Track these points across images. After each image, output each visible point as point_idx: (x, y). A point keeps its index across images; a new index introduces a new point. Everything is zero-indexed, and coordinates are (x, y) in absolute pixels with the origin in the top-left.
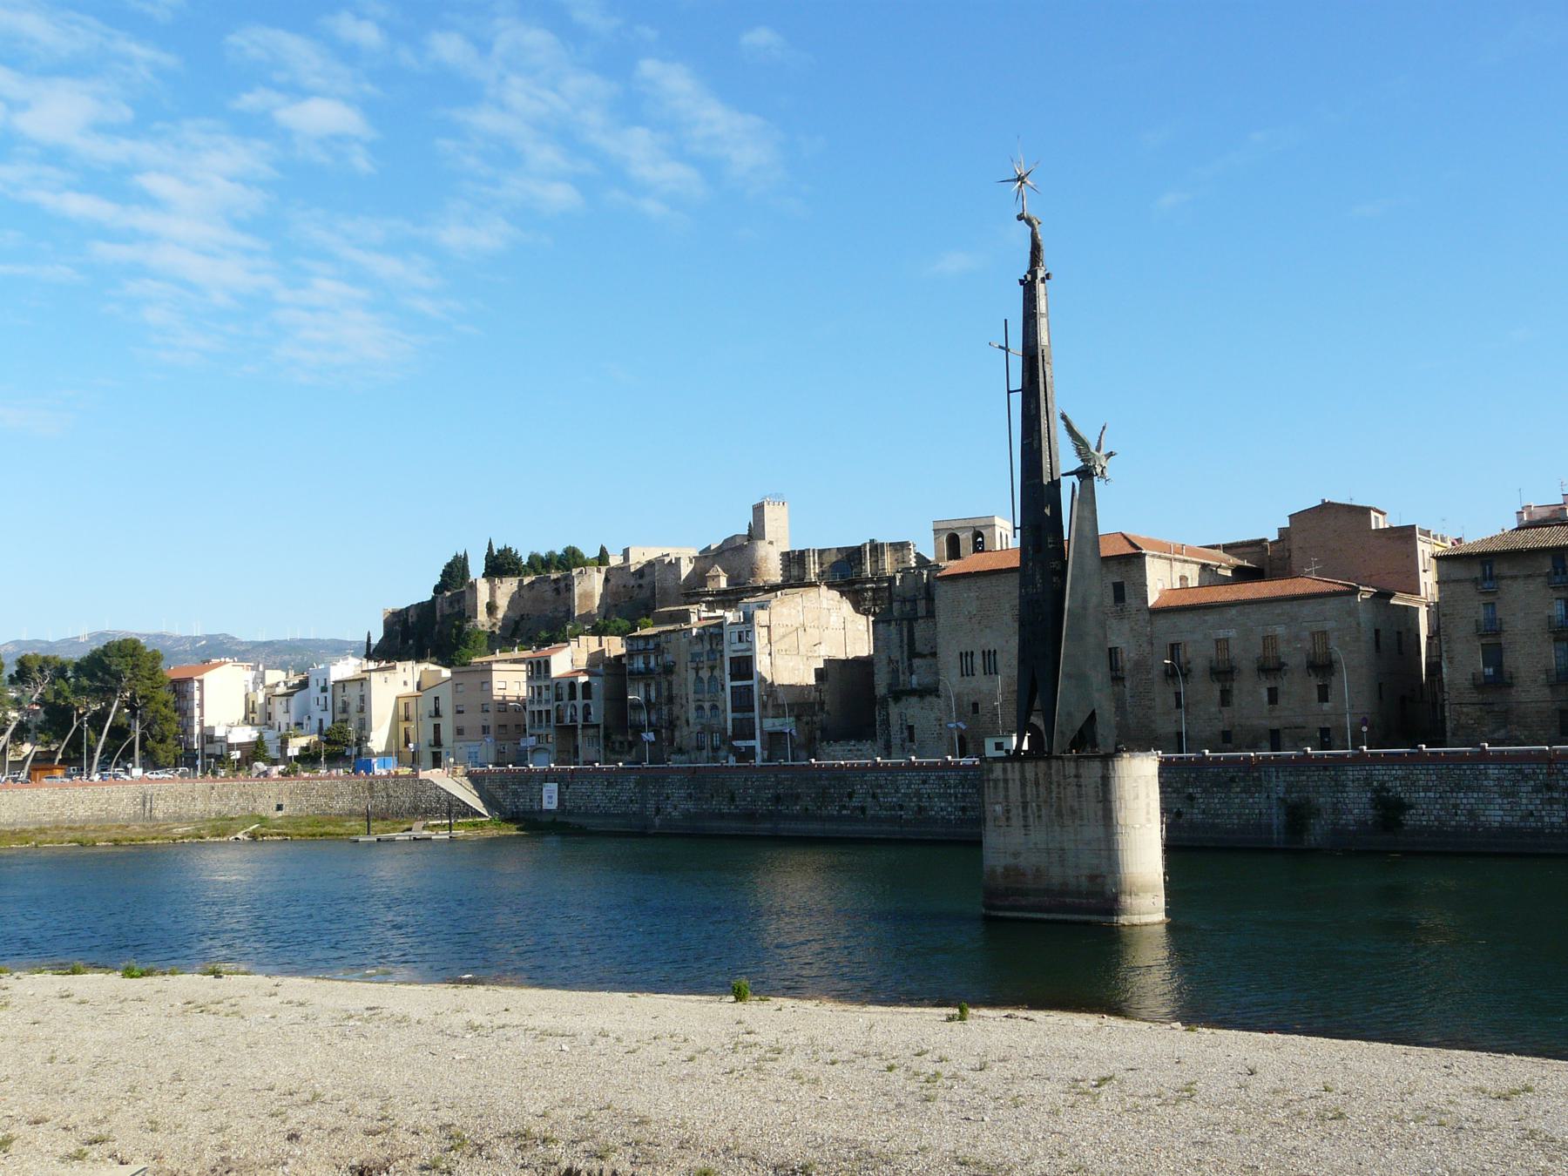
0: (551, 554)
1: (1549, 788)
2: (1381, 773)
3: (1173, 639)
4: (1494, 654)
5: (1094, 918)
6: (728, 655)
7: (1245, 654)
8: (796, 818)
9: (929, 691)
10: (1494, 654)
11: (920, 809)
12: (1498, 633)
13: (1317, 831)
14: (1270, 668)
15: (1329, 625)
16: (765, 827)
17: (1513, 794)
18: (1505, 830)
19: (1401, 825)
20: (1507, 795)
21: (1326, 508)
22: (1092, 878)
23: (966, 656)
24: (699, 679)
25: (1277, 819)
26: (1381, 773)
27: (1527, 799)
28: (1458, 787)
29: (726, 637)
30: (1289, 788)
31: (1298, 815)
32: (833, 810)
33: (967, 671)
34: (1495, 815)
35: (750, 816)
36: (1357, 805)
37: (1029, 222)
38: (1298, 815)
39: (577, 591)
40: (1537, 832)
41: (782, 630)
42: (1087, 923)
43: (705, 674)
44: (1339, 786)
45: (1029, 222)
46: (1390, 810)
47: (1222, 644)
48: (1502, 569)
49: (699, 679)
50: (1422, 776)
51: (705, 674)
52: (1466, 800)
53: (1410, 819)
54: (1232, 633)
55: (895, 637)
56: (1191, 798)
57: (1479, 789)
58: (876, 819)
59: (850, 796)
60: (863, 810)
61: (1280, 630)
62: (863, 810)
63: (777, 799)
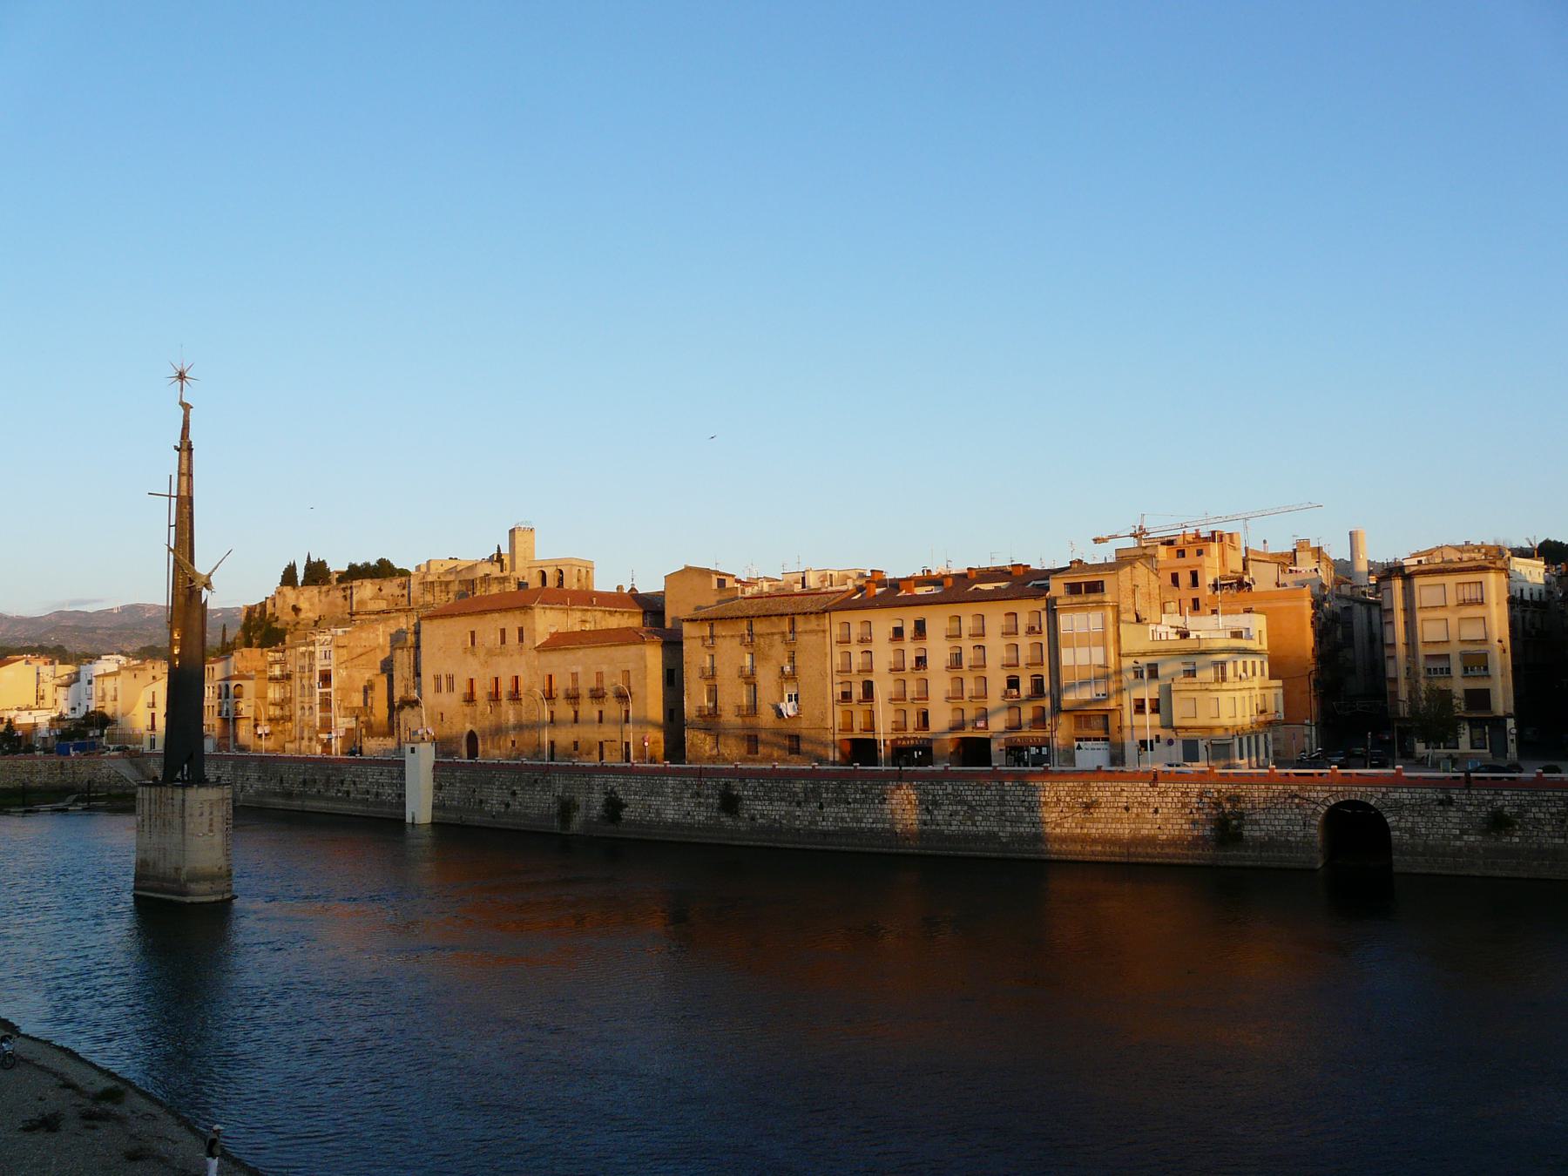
0: (367, 565)
1: (698, 795)
2: (614, 781)
3: (549, 672)
4: (713, 693)
5: (174, 898)
6: (318, 668)
7: (586, 685)
8: (312, 797)
9: (415, 703)
10: (713, 693)
11: (377, 794)
12: (713, 676)
13: (577, 823)
14: (597, 695)
15: (630, 666)
16: (296, 804)
17: (680, 799)
18: (676, 824)
19: (620, 819)
20: (676, 799)
21: (688, 570)
22: (177, 869)
23: (438, 678)
24: (303, 687)
25: (555, 809)
26: (614, 781)
27: (688, 803)
28: (651, 793)
29: (317, 654)
30: (566, 787)
31: (567, 808)
32: (332, 793)
33: (438, 689)
34: (670, 814)
35: (289, 795)
36: (598, 799)
37: (186, 407)
38: (567, 808)
39: (355, 598)
40: (691, 827)
41: (359, 651)
42: (171, 901)
43: (306, 682)
44: (590, 790)
45: (186, 407)
46: (614, 806)
47: (575, 676)
48: (719, 630)
49: (303, 687)
50: (635, 783)
51: (306, 682)
52: (655, 802)
53: (626, 814)
54: (579, 669)
55: (406, 660)
56: (514, 794)
57: (663, 794)
58: (356, 801)
59: (342, 782)
60: (348, 793)
61: (604, 668)
62: (348, 793)
63: (304, 782)
